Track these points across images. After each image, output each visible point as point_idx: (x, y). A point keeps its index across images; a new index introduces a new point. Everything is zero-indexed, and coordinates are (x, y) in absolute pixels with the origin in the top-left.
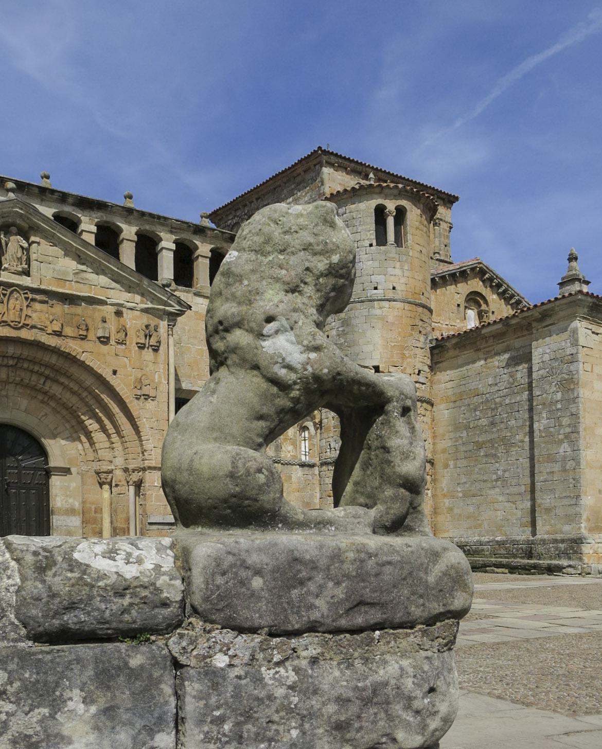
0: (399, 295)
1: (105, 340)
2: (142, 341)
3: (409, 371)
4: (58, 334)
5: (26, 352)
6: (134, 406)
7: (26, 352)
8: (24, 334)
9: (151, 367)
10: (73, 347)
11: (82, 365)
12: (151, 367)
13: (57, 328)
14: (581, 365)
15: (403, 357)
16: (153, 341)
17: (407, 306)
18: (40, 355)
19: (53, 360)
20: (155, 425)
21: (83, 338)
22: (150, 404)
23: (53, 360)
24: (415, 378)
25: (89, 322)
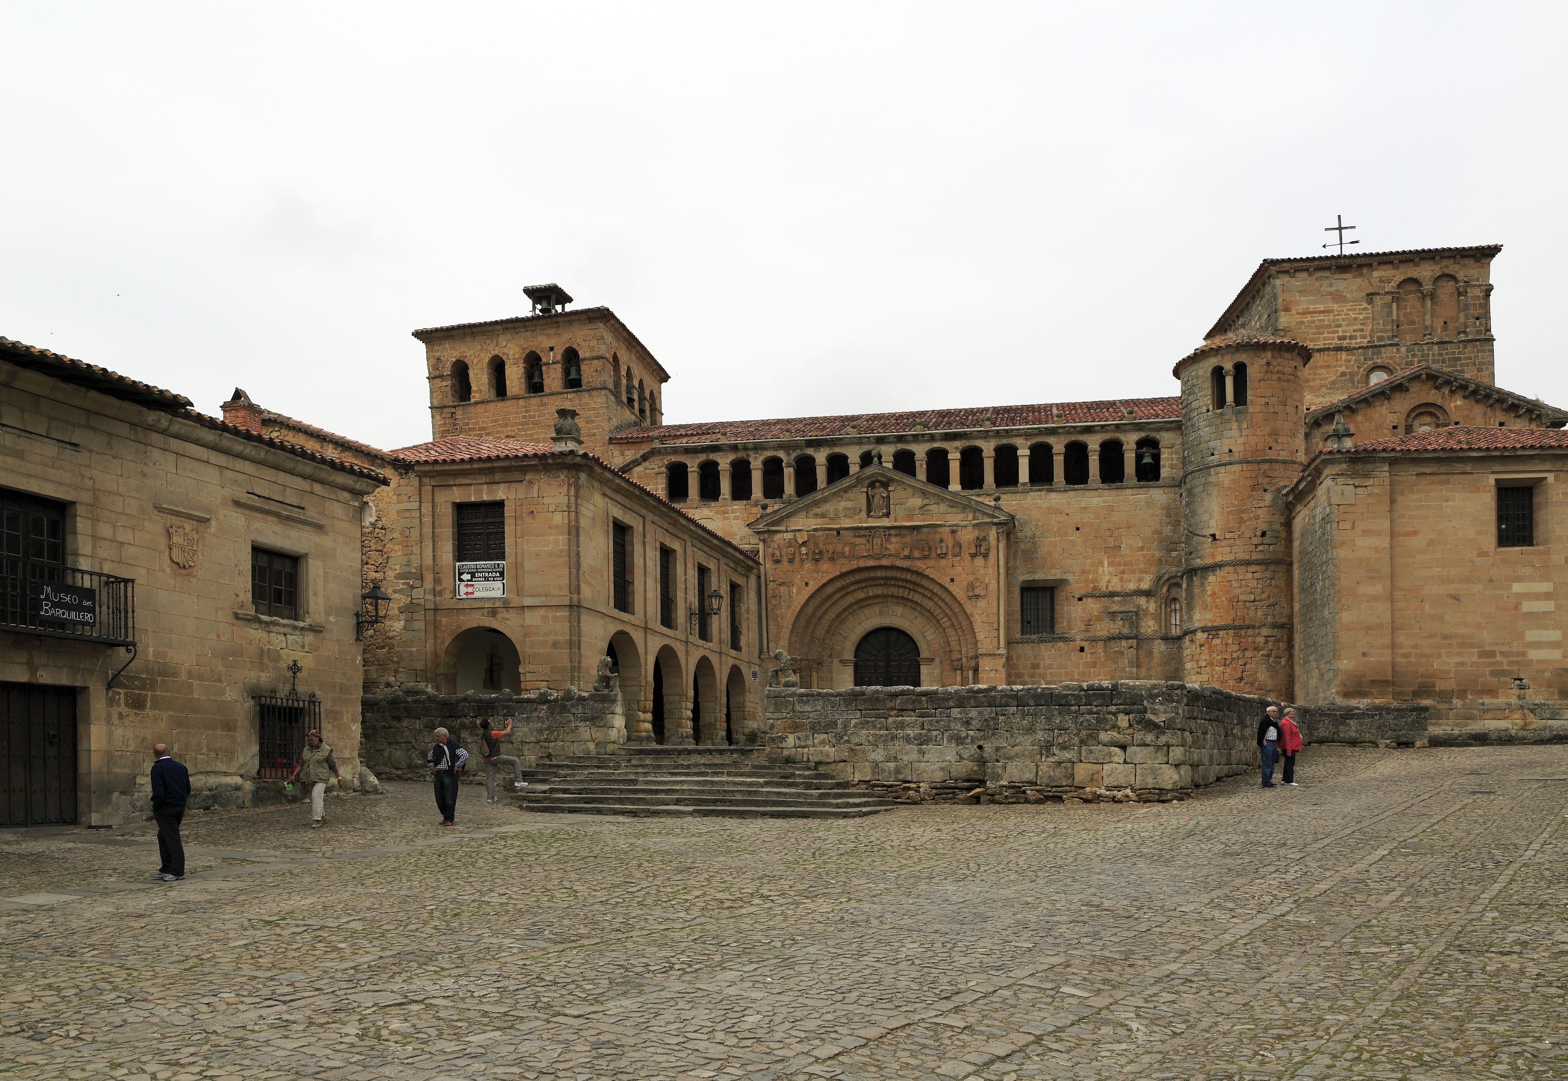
0: (1236, 457)
1: (943, 556)
2: (973, 551)
3: (1248, 534)
4: (907, 557)
5: (889, 574)
6: (968, 606)
7: (889, 574)
8: (885, 562)
9: (982, 571)
10: (920, 565)
11: (927, 577)
12: (982, 571)
13: (906, 553)
14: (1335, 525)
15: (1241, 521)
16: (983, 550)
17: (1245, 467)
18: (899, 574)
19: (909, 576)
20: (985, 619)
21: (926, 557)
22: (982, 603)
23: (909, 576)
24: (1256, 541)
25: (932, 543)
